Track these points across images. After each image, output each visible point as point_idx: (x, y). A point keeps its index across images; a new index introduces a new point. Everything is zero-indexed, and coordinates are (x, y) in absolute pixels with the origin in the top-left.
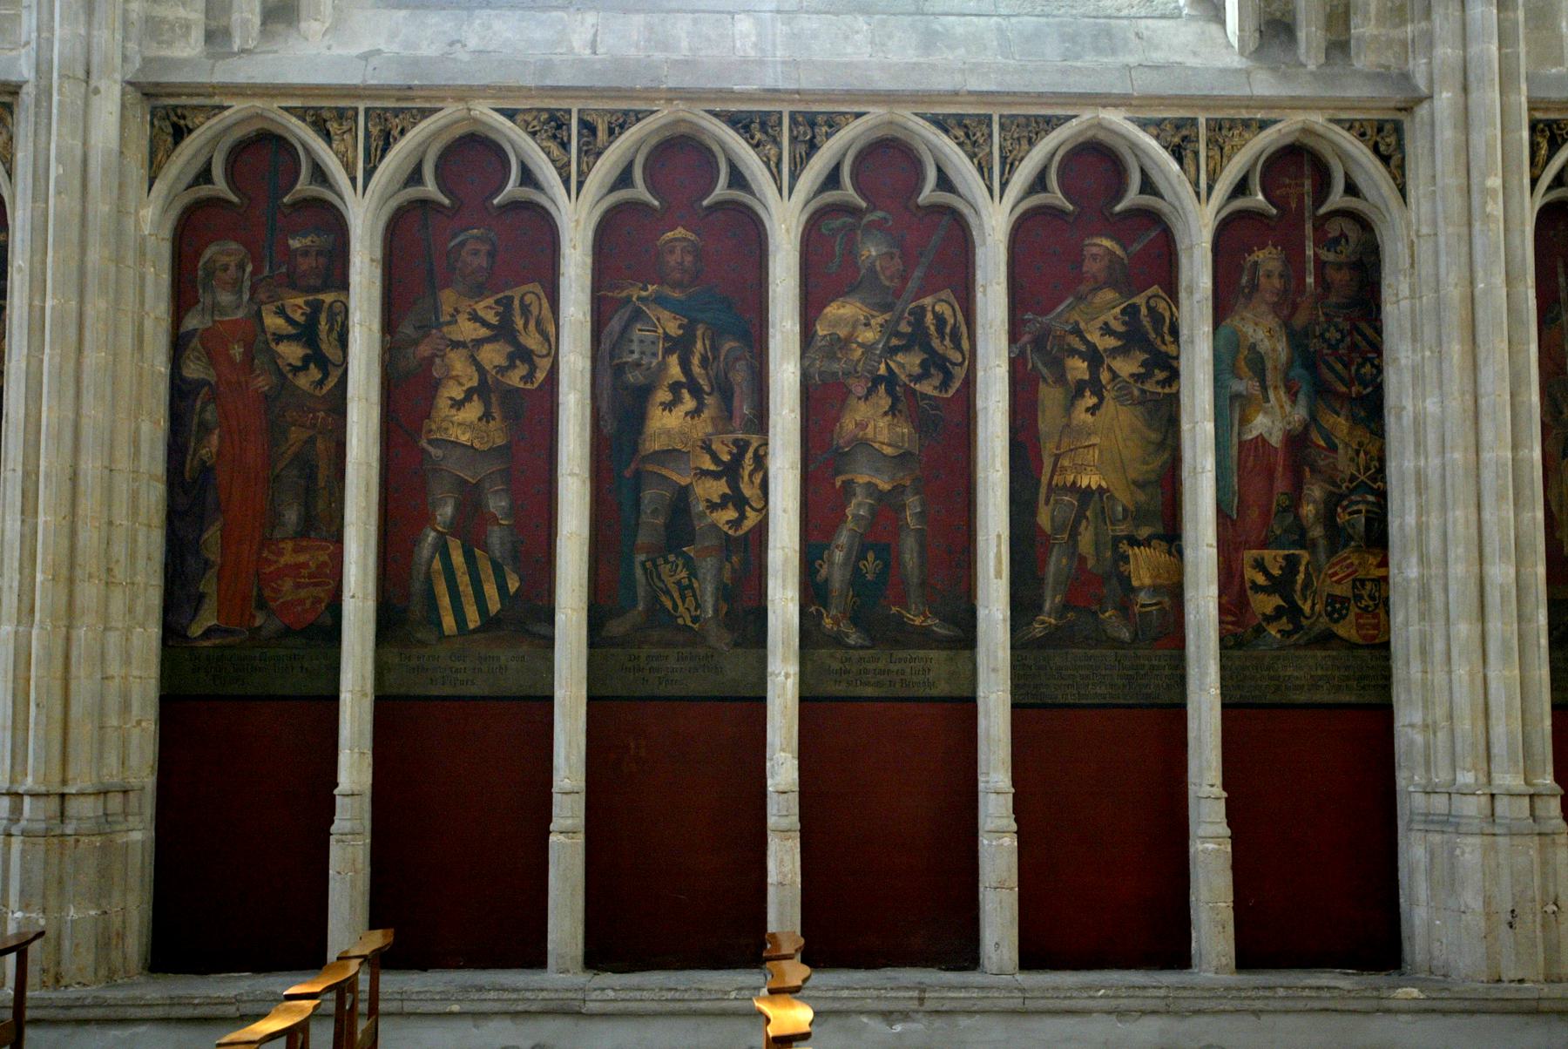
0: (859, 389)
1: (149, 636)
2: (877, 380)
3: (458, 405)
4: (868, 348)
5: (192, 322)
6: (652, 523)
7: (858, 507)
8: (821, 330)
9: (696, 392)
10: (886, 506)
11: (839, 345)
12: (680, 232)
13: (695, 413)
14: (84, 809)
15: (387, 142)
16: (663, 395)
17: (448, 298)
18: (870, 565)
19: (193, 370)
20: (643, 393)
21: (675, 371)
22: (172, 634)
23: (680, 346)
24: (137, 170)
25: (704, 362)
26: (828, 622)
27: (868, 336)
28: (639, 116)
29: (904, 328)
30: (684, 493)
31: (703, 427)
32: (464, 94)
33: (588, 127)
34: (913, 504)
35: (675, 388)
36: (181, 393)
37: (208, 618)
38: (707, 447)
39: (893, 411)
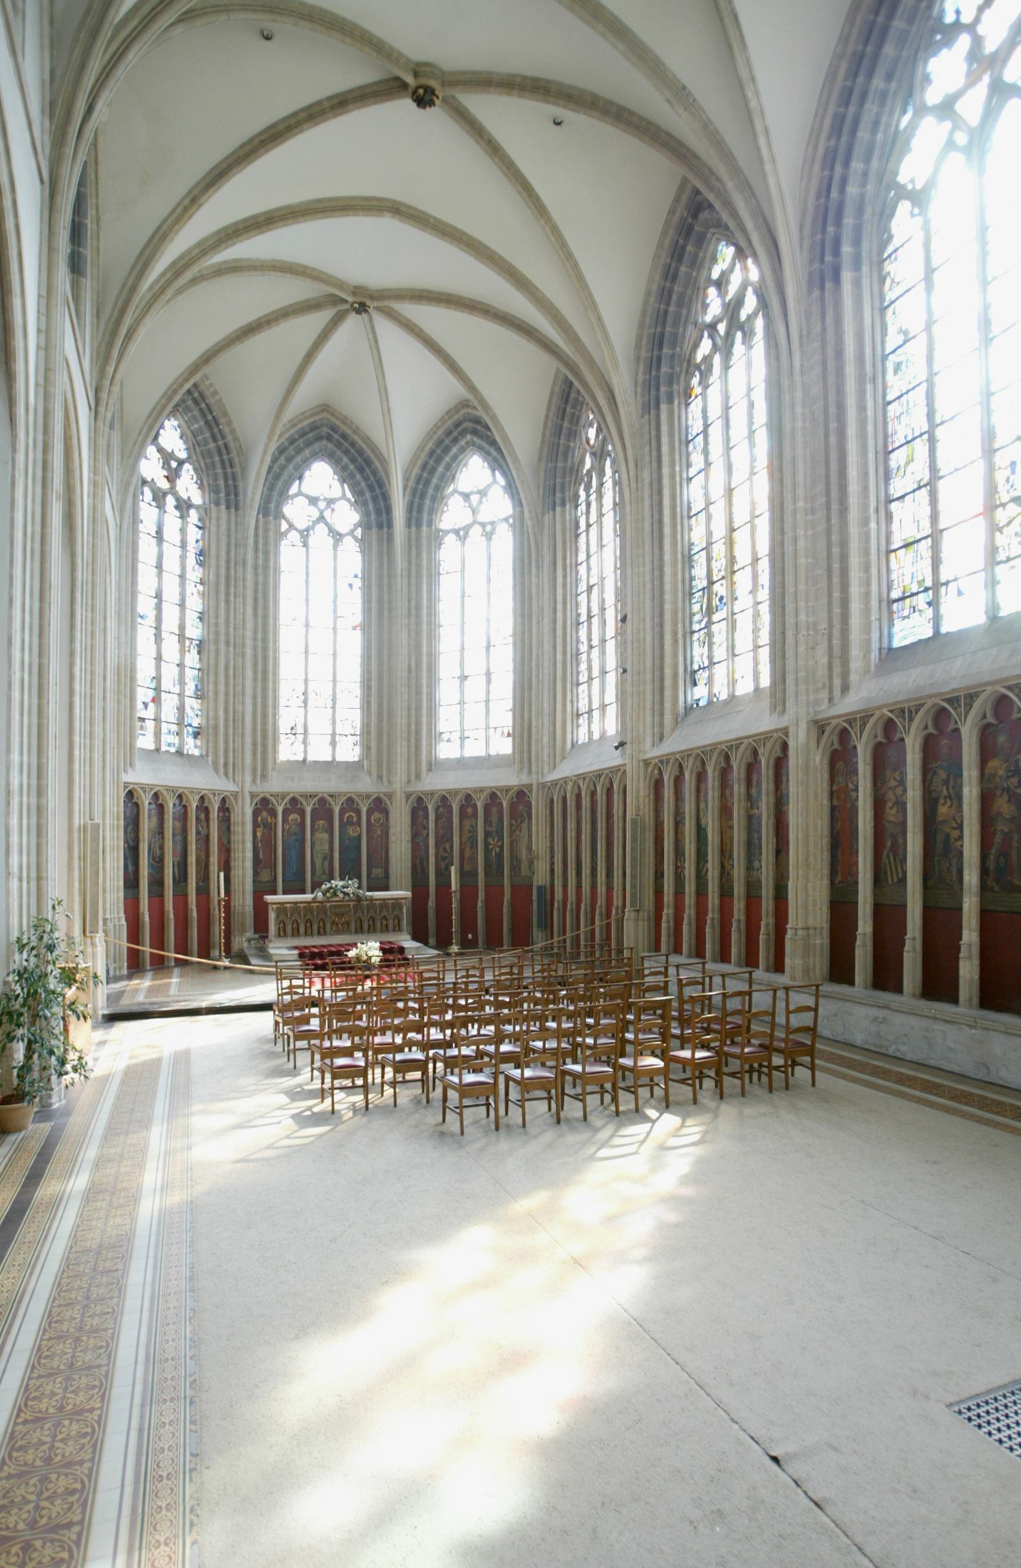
0: (998, 793)
1: (826, 882)
2: (1004, 790)
3: (891, 808)
4: (1001, 777)
5: (835, 788)
6: (939, 847)
7: (998, 839)
8: (987, 772)
9: (951, 799)
10: (1007, 837)
11: (993, 776)
12: (945, 741)
13: (950, 807)
14: (800, 932)
15: (865, 725)
16: (942, 801)
17: (888, 773)
18: (1002, 861)
19: (835, 802)
20: (936, 801)
21: (945, 792)
22: (832, 882)
23: (946, 782)
24: (813, 744)
25: (953, 787)
26: (989, 883)
27: (1001, 772)
28: (923, 705)
29: (1012, 768)
30: (948, 835)
31: (953, 812)
32: (880, 708)
33: (910, 712)
34: (1015, 837)
35: (945, 798)
36: (833, 809)
37: (839, 879)
38: (954, 819)
39: (1009, 801)
